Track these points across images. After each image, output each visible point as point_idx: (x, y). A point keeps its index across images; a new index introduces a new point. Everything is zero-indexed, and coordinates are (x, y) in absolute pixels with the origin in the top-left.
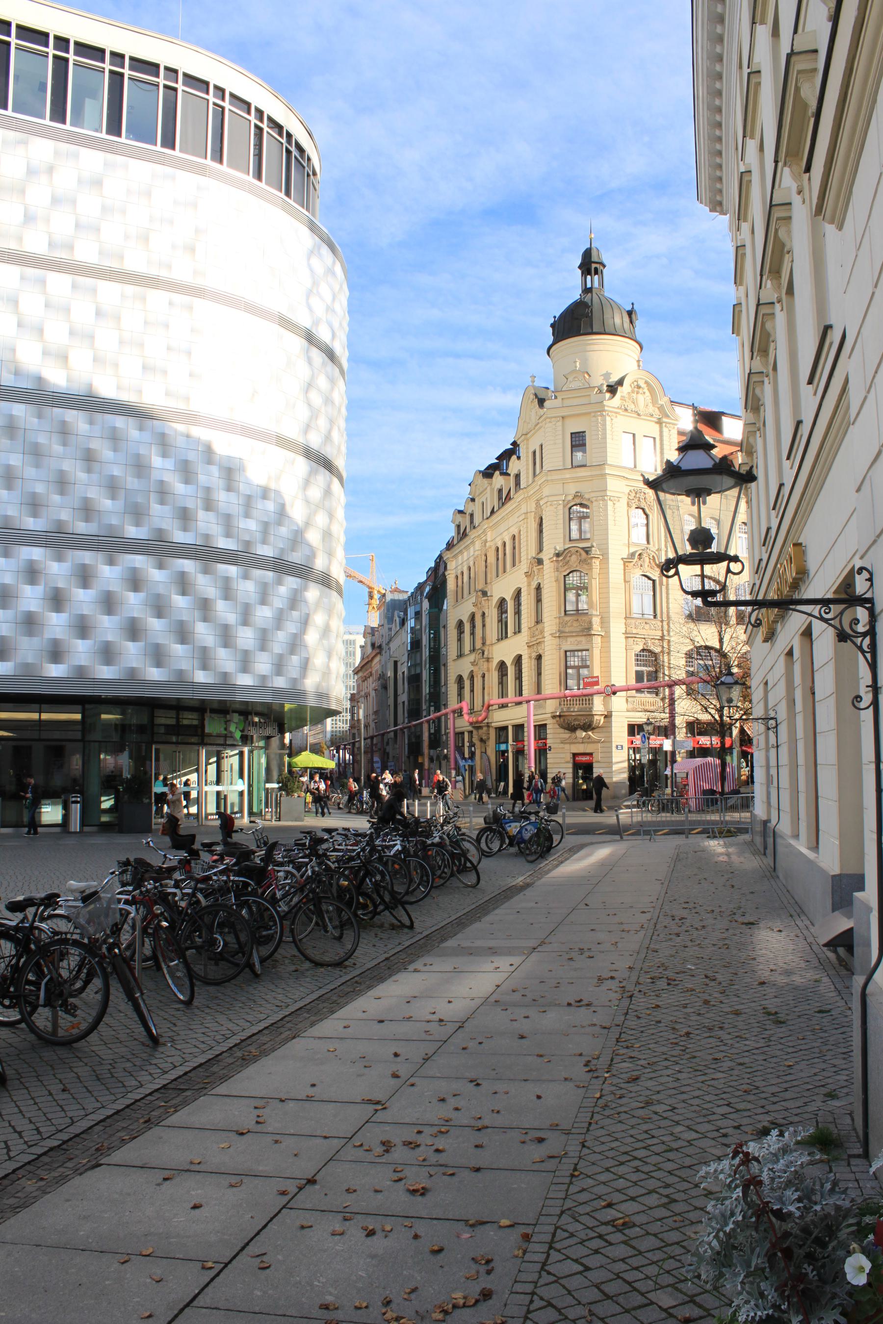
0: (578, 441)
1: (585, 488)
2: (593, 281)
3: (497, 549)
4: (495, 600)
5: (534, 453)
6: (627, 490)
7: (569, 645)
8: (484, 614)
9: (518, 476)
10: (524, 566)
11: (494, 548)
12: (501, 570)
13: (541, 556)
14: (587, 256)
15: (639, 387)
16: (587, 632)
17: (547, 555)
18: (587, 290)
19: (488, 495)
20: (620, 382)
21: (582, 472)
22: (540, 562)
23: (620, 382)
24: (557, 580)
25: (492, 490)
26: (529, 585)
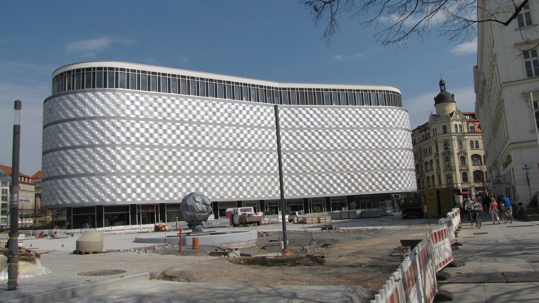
0: (445, 128)
1: (447, 138)
2: (443, 88)
3: (424, 150)
4: (424, 162)
5: (433, 129)
6: (456, 137)
7: (447, 173)
8: (421, 165)
9: (429, 134)
10: (433, 155)
11: (423, 149)
12: (426, 155)
13: (438, 153)
14: (441, 82)
15: (457, 114)
16: (451, 170)
17: (440, 153)
18: (442, 91)
19: (420, 136)
20: (453, 113)
21: (446, 135)
22: (438, 155)
23: (453, 113)
24: (443, 159)
25: (421, 136)
26: (435, 159)
